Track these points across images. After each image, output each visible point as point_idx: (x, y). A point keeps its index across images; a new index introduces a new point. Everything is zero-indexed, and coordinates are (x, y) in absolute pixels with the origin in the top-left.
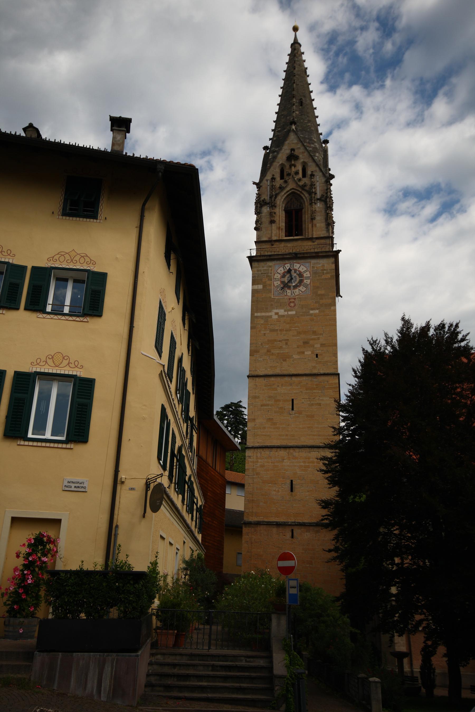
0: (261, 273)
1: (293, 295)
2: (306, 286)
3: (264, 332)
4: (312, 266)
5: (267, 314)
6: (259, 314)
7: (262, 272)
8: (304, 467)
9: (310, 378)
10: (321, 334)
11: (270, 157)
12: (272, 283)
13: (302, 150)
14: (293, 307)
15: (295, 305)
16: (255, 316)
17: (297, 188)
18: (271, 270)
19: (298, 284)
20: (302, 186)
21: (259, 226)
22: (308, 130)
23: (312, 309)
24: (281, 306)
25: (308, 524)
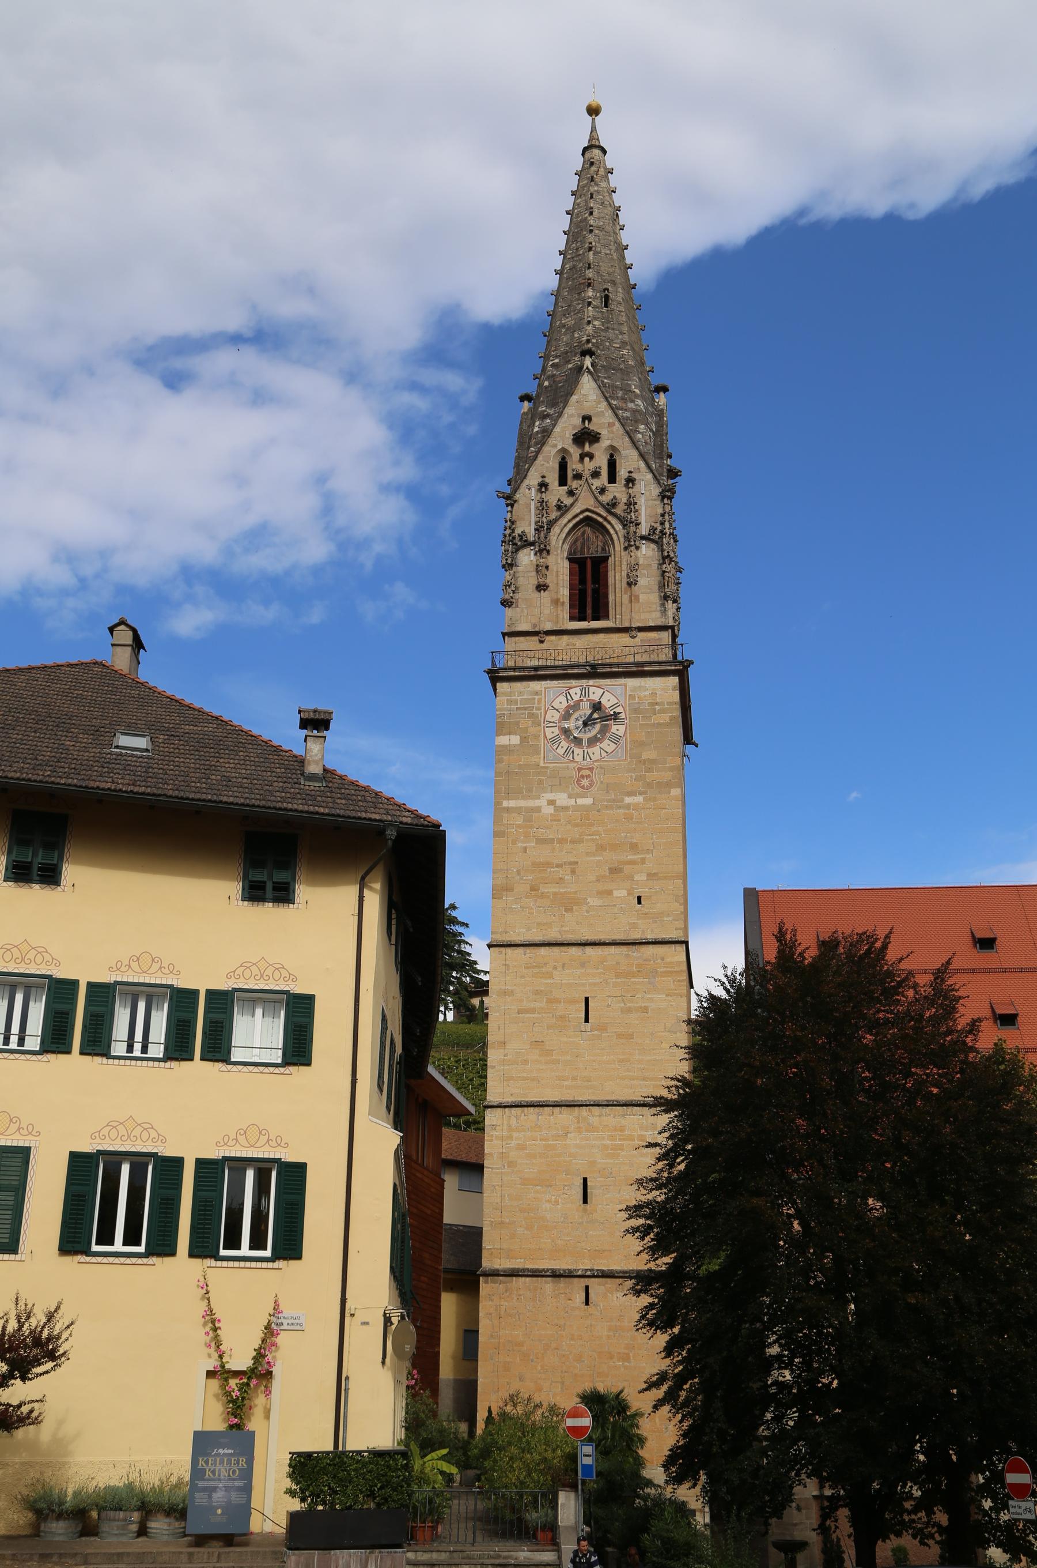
1: (588, 759)
2: (616, 740)
3: (525, 845)
4: (628, 693)
6: (512, 804)
8: (611, 1149)
9: (623, 949)
10: (648, 851)
11: (536, 429)
12: (540, 731)
13: (609, 416)
14: (588, 788)
15: (591, 785)
16: (504, 808)
17: (595, 510)
18: (539, 701)
19: (599, 736)
20: (608, 504)
21: (512, 597)
22: (622, 366)
23: (630, 794)
24: (560, 784)
25: (621, 1275)
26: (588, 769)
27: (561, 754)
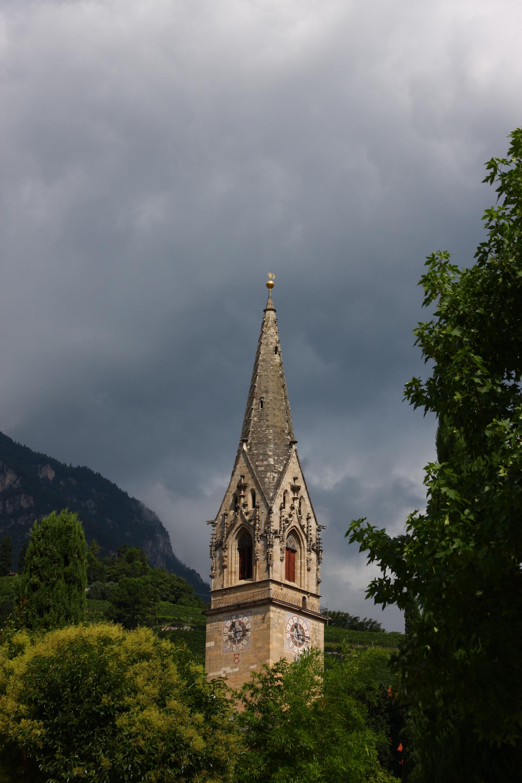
0: (214, 629)
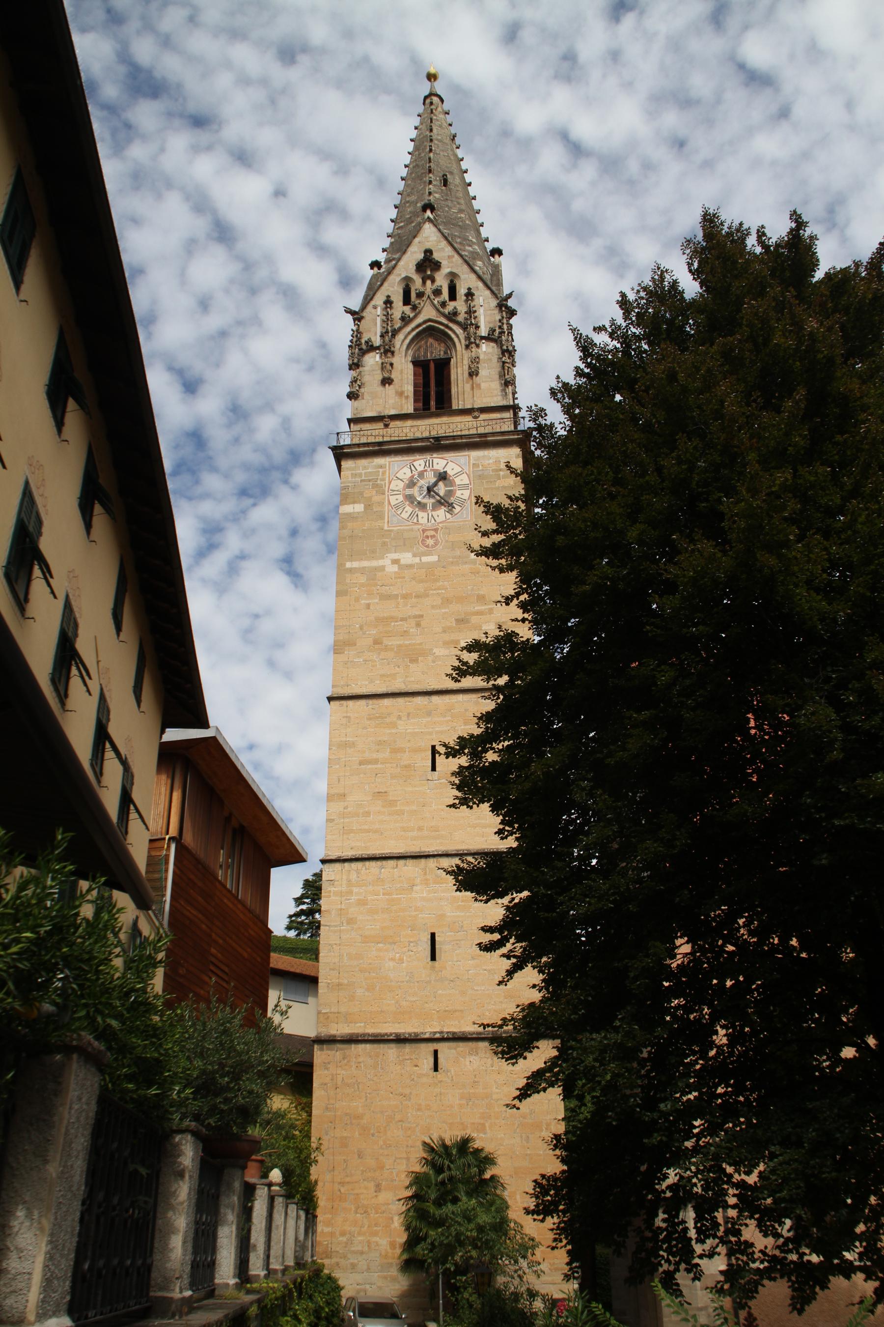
0: (361, 481)
1: (433, 521)
5: (375, 563)
6: (355, 564)
7: (363, 478)
12: (385, 499)
15: (436, 544)
16: (347, 569)
24: (405, 545)
26: (432, 530)
27: (406, 518)
